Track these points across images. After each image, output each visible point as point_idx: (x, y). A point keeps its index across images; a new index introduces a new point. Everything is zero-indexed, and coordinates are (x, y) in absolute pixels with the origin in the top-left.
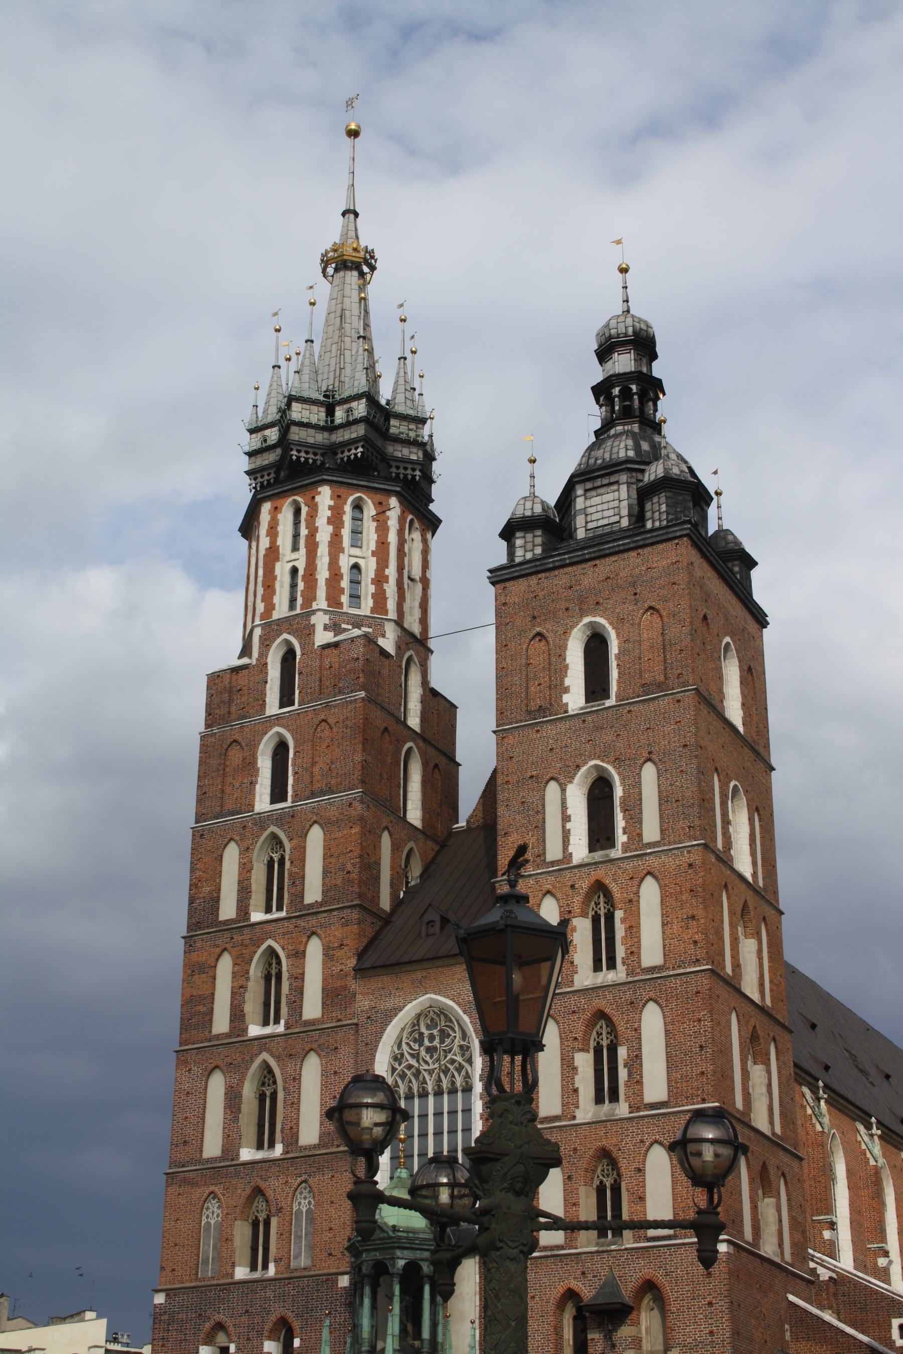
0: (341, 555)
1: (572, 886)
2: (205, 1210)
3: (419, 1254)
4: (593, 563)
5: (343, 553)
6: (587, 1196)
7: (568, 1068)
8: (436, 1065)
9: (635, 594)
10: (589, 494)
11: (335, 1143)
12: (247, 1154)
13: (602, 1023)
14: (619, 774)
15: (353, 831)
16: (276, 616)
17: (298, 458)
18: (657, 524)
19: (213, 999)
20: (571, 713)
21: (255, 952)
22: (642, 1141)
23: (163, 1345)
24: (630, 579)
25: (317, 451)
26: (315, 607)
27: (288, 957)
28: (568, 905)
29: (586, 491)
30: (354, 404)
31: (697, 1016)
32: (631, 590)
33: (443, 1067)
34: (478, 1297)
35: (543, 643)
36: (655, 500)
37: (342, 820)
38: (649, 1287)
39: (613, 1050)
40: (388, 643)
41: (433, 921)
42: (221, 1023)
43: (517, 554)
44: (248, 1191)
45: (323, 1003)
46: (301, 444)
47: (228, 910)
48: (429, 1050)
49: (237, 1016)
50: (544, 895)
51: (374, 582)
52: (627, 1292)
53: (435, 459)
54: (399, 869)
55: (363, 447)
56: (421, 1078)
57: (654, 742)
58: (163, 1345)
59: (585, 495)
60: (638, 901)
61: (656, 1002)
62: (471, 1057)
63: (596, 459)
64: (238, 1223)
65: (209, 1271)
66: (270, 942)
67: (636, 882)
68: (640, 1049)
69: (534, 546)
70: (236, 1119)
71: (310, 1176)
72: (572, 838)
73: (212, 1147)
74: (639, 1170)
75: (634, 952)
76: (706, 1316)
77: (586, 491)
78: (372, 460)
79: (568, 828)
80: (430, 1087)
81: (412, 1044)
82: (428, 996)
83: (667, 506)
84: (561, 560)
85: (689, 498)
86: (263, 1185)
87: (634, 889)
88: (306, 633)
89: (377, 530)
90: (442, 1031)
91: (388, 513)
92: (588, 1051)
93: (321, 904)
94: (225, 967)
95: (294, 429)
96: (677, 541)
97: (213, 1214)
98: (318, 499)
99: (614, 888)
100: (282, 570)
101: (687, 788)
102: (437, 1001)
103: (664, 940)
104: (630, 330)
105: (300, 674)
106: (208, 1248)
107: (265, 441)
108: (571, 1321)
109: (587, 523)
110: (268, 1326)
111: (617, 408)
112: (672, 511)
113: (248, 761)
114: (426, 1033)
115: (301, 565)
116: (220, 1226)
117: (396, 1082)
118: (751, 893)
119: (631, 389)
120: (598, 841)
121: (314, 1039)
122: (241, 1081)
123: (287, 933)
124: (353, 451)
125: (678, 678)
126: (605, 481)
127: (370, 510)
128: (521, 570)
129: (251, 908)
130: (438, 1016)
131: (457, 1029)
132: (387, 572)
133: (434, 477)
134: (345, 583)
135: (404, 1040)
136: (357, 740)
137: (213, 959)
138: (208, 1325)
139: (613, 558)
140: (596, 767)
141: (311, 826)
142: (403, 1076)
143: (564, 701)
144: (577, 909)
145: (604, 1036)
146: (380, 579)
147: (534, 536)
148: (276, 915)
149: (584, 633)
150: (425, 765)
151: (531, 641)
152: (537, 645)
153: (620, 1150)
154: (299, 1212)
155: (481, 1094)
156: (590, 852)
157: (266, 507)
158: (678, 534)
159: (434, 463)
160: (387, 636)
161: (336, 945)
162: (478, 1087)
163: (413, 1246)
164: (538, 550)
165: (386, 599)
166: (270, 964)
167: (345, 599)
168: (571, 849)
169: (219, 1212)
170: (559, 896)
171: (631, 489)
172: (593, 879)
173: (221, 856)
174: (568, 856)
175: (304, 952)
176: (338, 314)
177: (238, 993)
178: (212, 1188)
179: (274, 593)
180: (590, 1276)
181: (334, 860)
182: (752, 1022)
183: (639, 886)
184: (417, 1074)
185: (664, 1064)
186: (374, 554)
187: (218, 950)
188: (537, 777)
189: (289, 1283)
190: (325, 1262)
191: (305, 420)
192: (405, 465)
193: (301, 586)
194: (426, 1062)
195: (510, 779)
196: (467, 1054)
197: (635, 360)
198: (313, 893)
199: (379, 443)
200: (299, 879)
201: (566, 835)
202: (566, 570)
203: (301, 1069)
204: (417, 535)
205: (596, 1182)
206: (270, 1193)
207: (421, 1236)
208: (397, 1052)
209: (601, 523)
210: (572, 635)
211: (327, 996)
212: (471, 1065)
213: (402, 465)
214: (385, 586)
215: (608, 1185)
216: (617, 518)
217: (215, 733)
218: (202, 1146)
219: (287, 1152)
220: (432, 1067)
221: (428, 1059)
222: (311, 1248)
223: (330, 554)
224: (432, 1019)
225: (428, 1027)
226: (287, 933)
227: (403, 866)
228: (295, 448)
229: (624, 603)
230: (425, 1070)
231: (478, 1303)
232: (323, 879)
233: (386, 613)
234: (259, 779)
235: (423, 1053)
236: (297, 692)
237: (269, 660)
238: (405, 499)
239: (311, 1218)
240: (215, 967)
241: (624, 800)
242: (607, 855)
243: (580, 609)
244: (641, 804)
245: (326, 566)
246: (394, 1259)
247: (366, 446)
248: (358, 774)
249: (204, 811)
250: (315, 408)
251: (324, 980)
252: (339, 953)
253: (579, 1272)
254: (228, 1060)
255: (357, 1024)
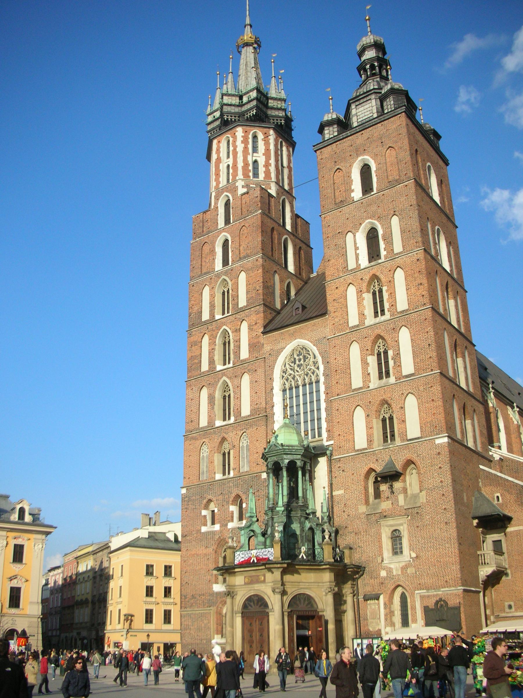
0: (248, 156)
1: (362, 279)
2: (201, 450)
3: (295, 457)
4: (361, 133)
5: (249, 155)
6: (377, 423)
7: (365, 363)
8: (303, 372)
9: (382, 142)
10: (357, 107)
11: (258, 413)
12: (219, 423)
13: (380, 340)
14: (380, 224)
15: (259, 271)
16: (221, 186)
17: (227, 119)
18: (390, 110)
19: (201, 356)
20: (355, 200)
21: (218, 333)
22: (402, 394)
23: (186, 511)
24: (379, 136)
25: (236, 115)
26: (237, 178)
27: (232, 332)
28: (360, 288)
29: (356, 106)
30: (251, 94)
31: (426, 330)
32: (380, 141)
33: (306, 373)
34: (327, 477)
35: (340, 173)
36: (388, 100)
37: (253, 268)
38: (409, 462)
39: (386, 353)
40: (273, 191)
41: (299, 308)
42: (205, 367)
43: (326, 137)
44: (220, 440)
45: (249, 351)
46: (228, 113)
47: (205, 316)
48: (298, 366)
49: (212, 362)
50: (349, 285)
51: (264, 166)
52: (399, 467)
53: (293, 121)
54: (283, 290)
55: (256, 110)
56: (296, 379)
57: (396, 206)
58: (186, 511)
59: (356, 108)
60: (394, 281)
61: (405, 326)
62: (318, 366)
63: (360, 93)
64: (216, 454)
65: (204, 477)
66: (225, 327)
67: (392, 272)
68: (399, 350)
69: (333, 132)
70: (213, 408)
71: (247, 430)
72: (360, 257)
73: (203, 422)
74: (402, 408)
75: (393, 305)
76: (438, 474)
77: (356, 106)
78: (261, 116)
79: (357, 253)
80: (300, 383)
81: (291, 364)
82: (296, 340)
83: (394, 101)
84: (346, 134)
85: (404, 98)
86: (226, 436)
87: (392, 276)
88: (234, 190)
89: (265, 144)
90: (304, 357)
91: (269, 137)
92: (374, 355)
93: (246, 307)
94: (206, 340)
95: (225, 107)
96: (399, 115)
97: (205, 451)
98: (236, 134)
99: (382, 277)
100: (223, 167)
101: (414, 224)
102: (301, 342)
103: (408, 297)
104: (372, 41)
105: (232, 208)
106: (204, 467)
107: (214, 117)
108: (372, 484)
109: (357, 119)
110: (231, 499)
111: (369, 73)
112: (396, 103)
113: (211, 250)
114: (297, 358)
115: (230, 162)
116: (208, 457)
117: (284, 383)
118: (450, 278)
119: (375, 65)
120: (373, 257)
121: (246, 367)
122: (214, 391)
123: (232, 322)
124: (252, 113)
125: (405, 176)
126: (365, 100)
127: (260, 136)
128: (328, 142)
129: (215, 313)
130: (302, 349)
131: (311, 354)
132: (270, 162)
133: (293, 128)
134: (251, 168)
135: (287, 364)
136: (259, 232)
137: (200, 339)
138: (205, 501)
139: (370, 129)
140: (369, 222)
141: (240, 273)
142: (287, 380)
143: (352, 196)
144: (364, 290)
145: (381, 347)
146: (267, 165)
147: (333, 128)
148: (226, 315)
149: (359, 165)
150: (295, 246)
151: (335, 172)
152: (338, 174)
153: (392, 399)
154: (243, 446)
155: (324, 382)
156: (369, 263)
157: (215, 142)
158: (400, 112)
159: (293, 123)
160: (272, 189)
161: (254, 323)
162: (322, 379)
163: (292, 453)
164: (336, 134)
165: (270, 173)
166: (225, 338)
167: (251, 174)
168: (360, 262)
169: (208, 450)
170: (355, 284)
171: (377, 101)
172: (371, 274)
173: (202, 293)
174: (358, 265)
175: (240, 329)
176: (245, 64)
177: (211, 352)
178: (204, 440)
179: (220, 177)
180: (380, 461)
181: (251, 286)
182: (455, 337)
183: (394, 274)
184: (294, 376)
185: (412, 356)
186: (264, 154)
187: (202, 334)
188: (342, 232)
189: (240, 479)
190: (256, 468)
191: (230, 103)
192: (277, 118)
193: (231, 171)
194: (297, 371)
195: (329, 235)
196: (317, 366)
197: (376, 53)
198: (242, 302)
199: (264, 109)
200: (236, 297)
201: (357, 256)
202: (349, 138)
203: (241, 382)
204: (284, 149)
205: (382, 417)
206: (229, 439)
207: (296, 448)
208: (284, 368)
209: (364, 118)
210: (354, 166)
211: (251, 347)
212: (319, 370)
213: (275, 119)
214: (270, 168)
215: (387, 417)
216: (372, 114)
217: (197, 241)
218: (199, 422)
219: (236, 420)
220: (300, 373)
221: (298, 369)
222: (249, 462)
223: (243, 156)
224: (300, 352)
225: (298, 355)
226: (232, 322)
227: (286, 289)
228: (226, 115)
229: (377, 147)
230: (297, 375)
231: (327, 480)
232: (247, 295)
233: (271, 179)
234: (217, 257)
235: (296, 368)
236: (231, 216)
237: (219, 205)
238: (278, 132)
239: (248, 449)
240: (201, 342)
241: (384, 236)
242: (377, 262)
243: (357, 154)
244: (392, 235)
245: (242, 161)
246: (282, 459)
247: (257, 109)
248: (260, 246)
249: (194, 275)
250: (234, 98)
251: (249, 340)
252: (255, 327)
253: (375, 460)
254: (208, 382)
255: (265, 358)
